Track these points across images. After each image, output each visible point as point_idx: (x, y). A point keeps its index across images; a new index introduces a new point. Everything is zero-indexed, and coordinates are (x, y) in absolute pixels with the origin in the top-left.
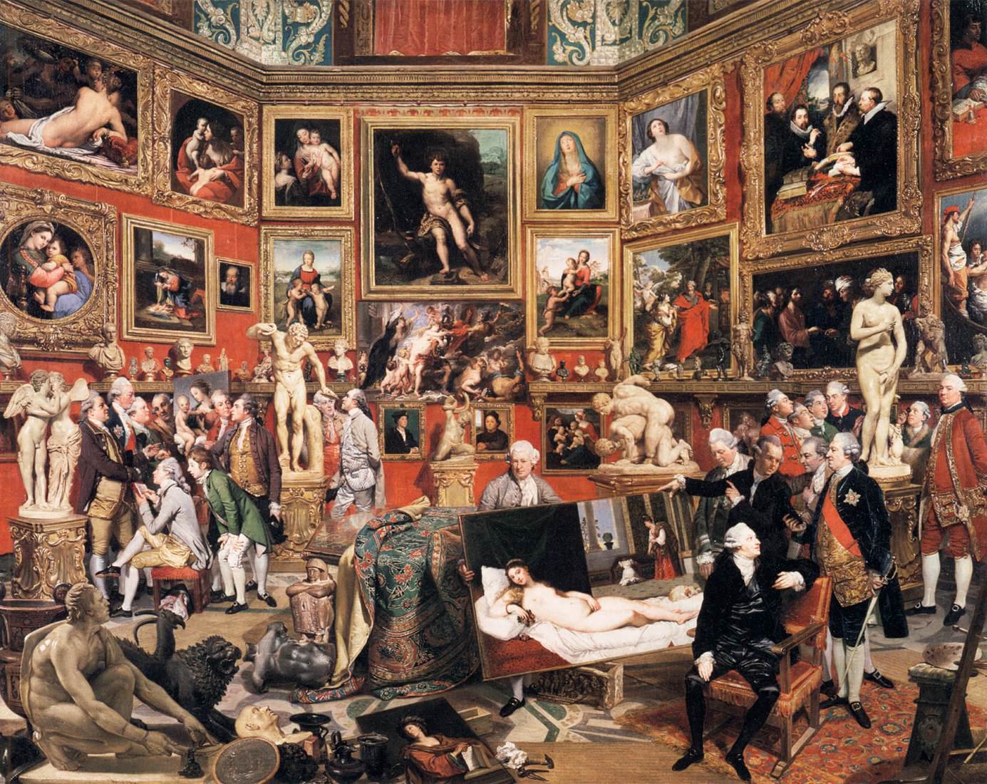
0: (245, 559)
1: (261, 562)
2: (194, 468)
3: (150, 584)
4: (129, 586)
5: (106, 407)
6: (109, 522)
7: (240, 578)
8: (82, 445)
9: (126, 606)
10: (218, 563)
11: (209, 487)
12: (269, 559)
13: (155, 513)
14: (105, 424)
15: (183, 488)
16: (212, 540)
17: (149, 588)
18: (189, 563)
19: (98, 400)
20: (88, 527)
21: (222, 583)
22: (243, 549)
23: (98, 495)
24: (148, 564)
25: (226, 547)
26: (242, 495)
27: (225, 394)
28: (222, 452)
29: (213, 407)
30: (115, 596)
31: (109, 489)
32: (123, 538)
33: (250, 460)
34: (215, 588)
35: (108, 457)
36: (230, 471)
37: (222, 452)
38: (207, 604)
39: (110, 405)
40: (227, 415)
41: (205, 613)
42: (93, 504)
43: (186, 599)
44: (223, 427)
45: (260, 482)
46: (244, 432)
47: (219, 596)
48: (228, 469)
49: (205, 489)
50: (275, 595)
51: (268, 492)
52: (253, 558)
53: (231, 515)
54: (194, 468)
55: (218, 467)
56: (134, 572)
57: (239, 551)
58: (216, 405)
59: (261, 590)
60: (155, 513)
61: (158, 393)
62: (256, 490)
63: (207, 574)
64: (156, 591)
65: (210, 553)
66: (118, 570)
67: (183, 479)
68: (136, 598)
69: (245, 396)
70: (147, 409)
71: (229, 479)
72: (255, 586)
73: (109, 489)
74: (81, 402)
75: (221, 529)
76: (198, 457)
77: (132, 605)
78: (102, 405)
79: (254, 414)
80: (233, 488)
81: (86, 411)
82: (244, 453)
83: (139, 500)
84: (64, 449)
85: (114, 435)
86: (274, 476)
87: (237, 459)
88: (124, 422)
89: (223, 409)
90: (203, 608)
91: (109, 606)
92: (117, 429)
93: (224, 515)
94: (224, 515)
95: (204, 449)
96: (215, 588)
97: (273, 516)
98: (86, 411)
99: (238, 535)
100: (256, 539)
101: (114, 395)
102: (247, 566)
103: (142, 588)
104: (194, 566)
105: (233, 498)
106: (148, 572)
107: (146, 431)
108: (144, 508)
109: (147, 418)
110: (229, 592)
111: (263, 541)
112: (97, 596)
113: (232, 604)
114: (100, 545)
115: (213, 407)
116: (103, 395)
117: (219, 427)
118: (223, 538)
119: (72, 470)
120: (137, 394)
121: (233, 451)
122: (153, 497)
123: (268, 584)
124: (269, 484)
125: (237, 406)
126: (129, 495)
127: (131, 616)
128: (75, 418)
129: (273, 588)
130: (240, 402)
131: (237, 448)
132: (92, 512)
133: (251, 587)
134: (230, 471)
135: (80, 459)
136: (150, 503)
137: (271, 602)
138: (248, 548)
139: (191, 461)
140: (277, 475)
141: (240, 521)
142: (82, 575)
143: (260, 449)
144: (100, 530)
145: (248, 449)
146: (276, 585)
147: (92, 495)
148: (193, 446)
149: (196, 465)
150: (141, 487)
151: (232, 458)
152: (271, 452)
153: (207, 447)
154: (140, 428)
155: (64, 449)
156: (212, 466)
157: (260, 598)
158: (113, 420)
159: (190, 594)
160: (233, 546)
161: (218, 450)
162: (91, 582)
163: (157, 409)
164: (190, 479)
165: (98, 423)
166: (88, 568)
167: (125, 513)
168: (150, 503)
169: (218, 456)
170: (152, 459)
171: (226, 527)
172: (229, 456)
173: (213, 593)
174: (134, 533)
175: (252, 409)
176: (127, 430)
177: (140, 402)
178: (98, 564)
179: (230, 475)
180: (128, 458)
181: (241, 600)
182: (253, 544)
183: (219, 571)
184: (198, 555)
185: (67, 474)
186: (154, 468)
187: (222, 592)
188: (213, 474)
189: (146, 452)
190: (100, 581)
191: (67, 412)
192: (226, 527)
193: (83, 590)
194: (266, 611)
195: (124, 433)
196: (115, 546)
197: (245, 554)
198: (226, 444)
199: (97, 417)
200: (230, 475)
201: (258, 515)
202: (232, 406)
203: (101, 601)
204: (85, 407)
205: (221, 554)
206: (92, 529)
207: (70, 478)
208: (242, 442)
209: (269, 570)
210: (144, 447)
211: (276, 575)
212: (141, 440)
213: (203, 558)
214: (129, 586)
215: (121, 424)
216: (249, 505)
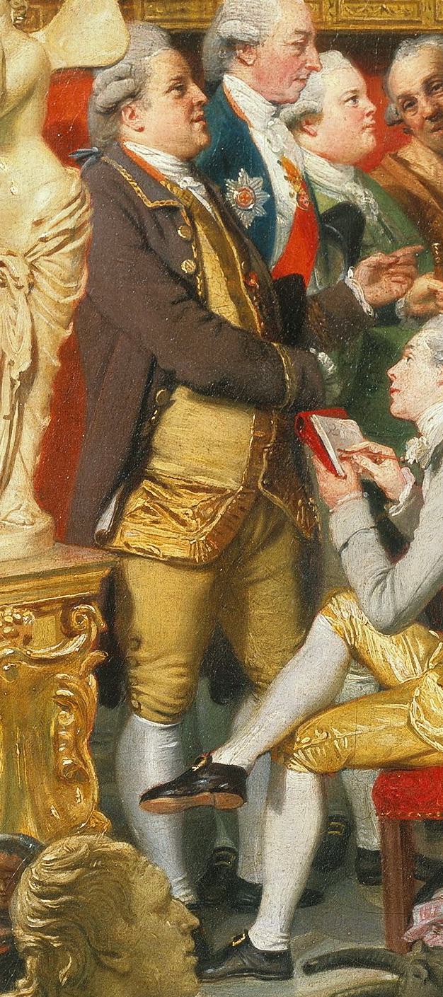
3: (370, 837)
4: (283, 845)
5: (195, 93)
6: (200, 580)
8: (88, 255)
9: (267, 933)
13: (395, 542)
14: (191, 164)
17: (363, 853)
19: (162, 65)
20: (114, 598)
23: (157, 465)
24: (364, 754)
30: (223, 890)
31: (203, 440)
32: (254, 652)
35: (203, 302)
39: (213, 87)
42: (137, 501)
56: (301, 785)
60: (395, 542)
61: (414, 36)
64: (392, 871)
66: (235, 778)
68: (309, 898)
70: (365, 104)
73: (203, 440)
74: (88, 72)
77: (293, 926)
78: (179, 87)
81: (113, 111)
83: (327, 483)
84: (18, 269)
85: (227, 212)
88: (270, 158)
91: (196, 933)
92: (240, 187)
98: (113, 111)
101: (231, 44)
103: (334, 856)
106: (362, 785)
107: (362, 197)
108: (349, 521)
109: (367, 141)
112: (146, 891)
114: (160, 676)
116: (187, 43)
119: (50, 358)
120: (325, 41)
122: (387, 474)
126: (287, 463)
127: (287, 975)
128: (66, 140)
132: (133, 534)
135: (81, 314)
136: (376, 496)
142: (83, 802)
144: (163, 608)
147: (134, 465)
150: (339, 432)
154: (337, 185)
155: (18, 269)
158: (226, 152)
162: (122, 829)
163: (409, 101)
165: (163, 162)
166: (108, 771)
167: (272, 536)
168: (376, 496)
170: (386, 313)
174: (305, 622)
176: (284, 190)
177: (336, 77)
178: (151, 754)
180: (287, 310)
185: (28, 378)
186: (392, 353)
189: (361, 285)
190: (159, 829)
191: (31, 117)
193: (90, 862)
195: (270, 205)
196: (225, 677)
199: (157, 137)
203: (162, 908)
204: (106, 91)
206: (130, 609)
207: (40, 393)
210: (353, 261)
212: (338, 231)
214: (283, 845)
215: (256, 166)
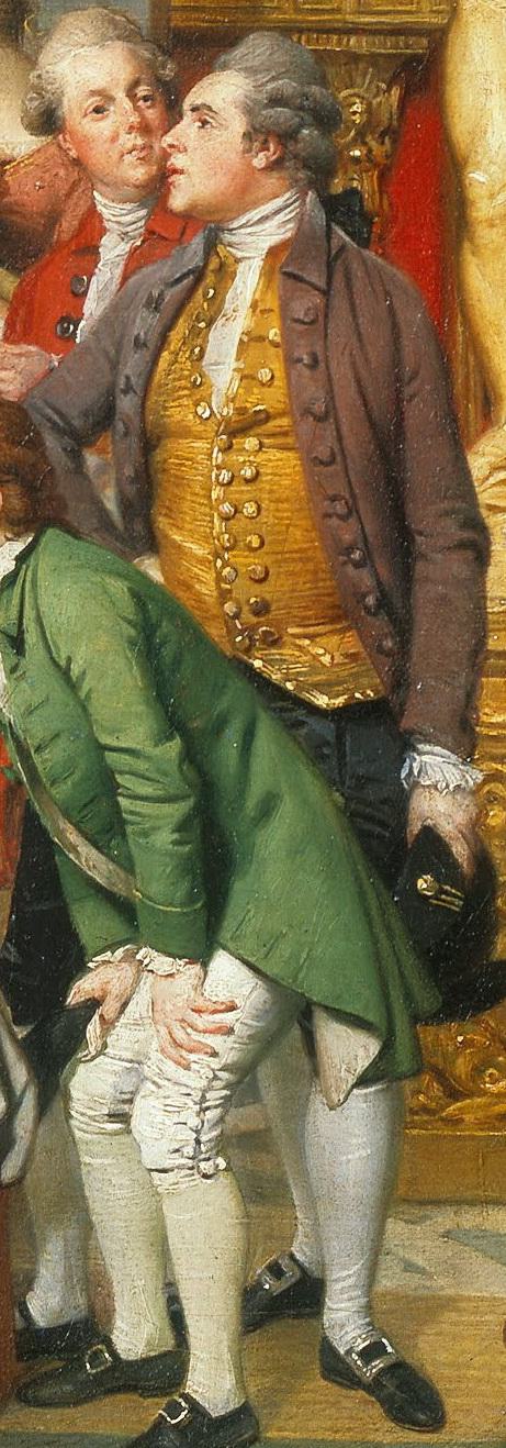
0: (245, 1118)
1: (347, 1136)
7: (206, 1235)
10: (68, 1143)
12: (400, 1124)
21: (92, 1280)
22: (229, 1050)
25: (124, 1039)
26: (234, 697)
27: (129, 35)
28: (105, 417)
29: (47, 121)
33: (282, 467)
34: (46, 1304)
36: (151, 543)
37: (105, 417)
40: (139, 173)
44: (113, 251)
45: (340, 612)
46: (247, 283)
48: (138, 525)
50: (434, 1354)
51: (399, 681)
52: (296, 1112)
53: (158, 827)
55: (76, 512)
57: (203, 1067)
58: (73, 105)
59: (344, 1322)
62: (319, 663)
69: (257, 48)
71: (143, 593)
72: (306, 1294)
75: (89, 921)
79: (317, 172)
80: (164, 640)
82: (241, 426)
86: (438, 569)
87: (196, 458)
89: (110, 136)
93: (109, 831)
94: (109, 831)
96: (46, 1304)
97: (429, 834)
99: (202, 958)
100: (317, 988)
105: (172, 722)
111: (363, 1001)
113: (155, 1409)
115: (47, 121)
117: (87, 250)
118: (100, 978)
121: (179, 413)
123: (385, 1283)
124: (403, 628)
125: (204, 115)
129: (429, 1308)
130: (224, 91)
131: (198, 388)
133: (280, 1302)
134: (151, 543)
138: (264, 1044)
140: (458, 566)
143: (346, 395)
145: (273, 399)
146: (443, 1285)
151: (173, 452)
152: (421, 412)
157: (335, 1368)
161: (77, 402)
169: (78, 441)
171: (126, 910)
172: (149, 441)
173: (35, 1343)
175: (295, 138)
179: (152, 569)
181: (212, 1381)
182: (293, 1017)
183: (72, 1199)
187: (90, 1329)
188: (44, 562)
192: (126, 910)
197: (243, 1082)
198: (132, 364)
200: (152, 569)
201: (332, 824)
202: (173, 113)
205: (90, 1083)
208: (233, 351)
209: (399, 1192)
211: (444, 1219)
216: (270, 764)
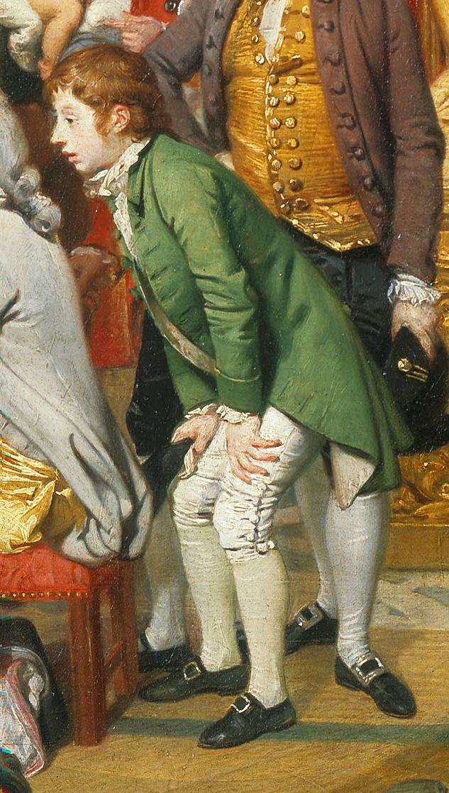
1: (353, 527)
2: (78, 129)
7: (262, 591)
11: (138, 208)
15: (28, 215)
16: (148, 435)
18: (52, 527)
21: (188, 620)
25: (208, 464)
28: (196, 62)
34: (158, 635)
38: (123, 703)
41: (117, 742)
43: (35, 683)
47: (174, 669)
48: (218, 132)
49: (122, 218)
54: (78, 129)
59: (351, 647)
63: (120, 582)
65: (141, 487)
67: (32, 177)
75: (186, 388)
76: (94, 84)
80: (234, 206)
90: (103, 722)
93: (199, 330)
95: (119, 51)
96: (158, 635)
97: (406, 333)
102: (294, 535)
104: (73, 546)
105: (240, 260)
110: (215, 654)
111: (364, 440)
123: (377, 622)
129: (405, 638)
133: (310, 635)
137: (393, 695)
139: (64, 99)
141: (266, 353)
148: (73, 34)
149: (87, 116)
152: (400, 60)
153: (134, 41)
156: (152, 121)
159: (53, 668)
160: (235, 460)
161: (178, 52)
164: (59, 175)
171: (209, 381)
172: (225, 79)
179: (227, 161)
181: (265, 686)
182: (318, 451)
184: (90, 500)
187: (186, 652)
194: (369, 733)
197: (285, 492)
198: (214, 29)
200: (227, 161)
205: (186, 493)
213: (109, 508)
